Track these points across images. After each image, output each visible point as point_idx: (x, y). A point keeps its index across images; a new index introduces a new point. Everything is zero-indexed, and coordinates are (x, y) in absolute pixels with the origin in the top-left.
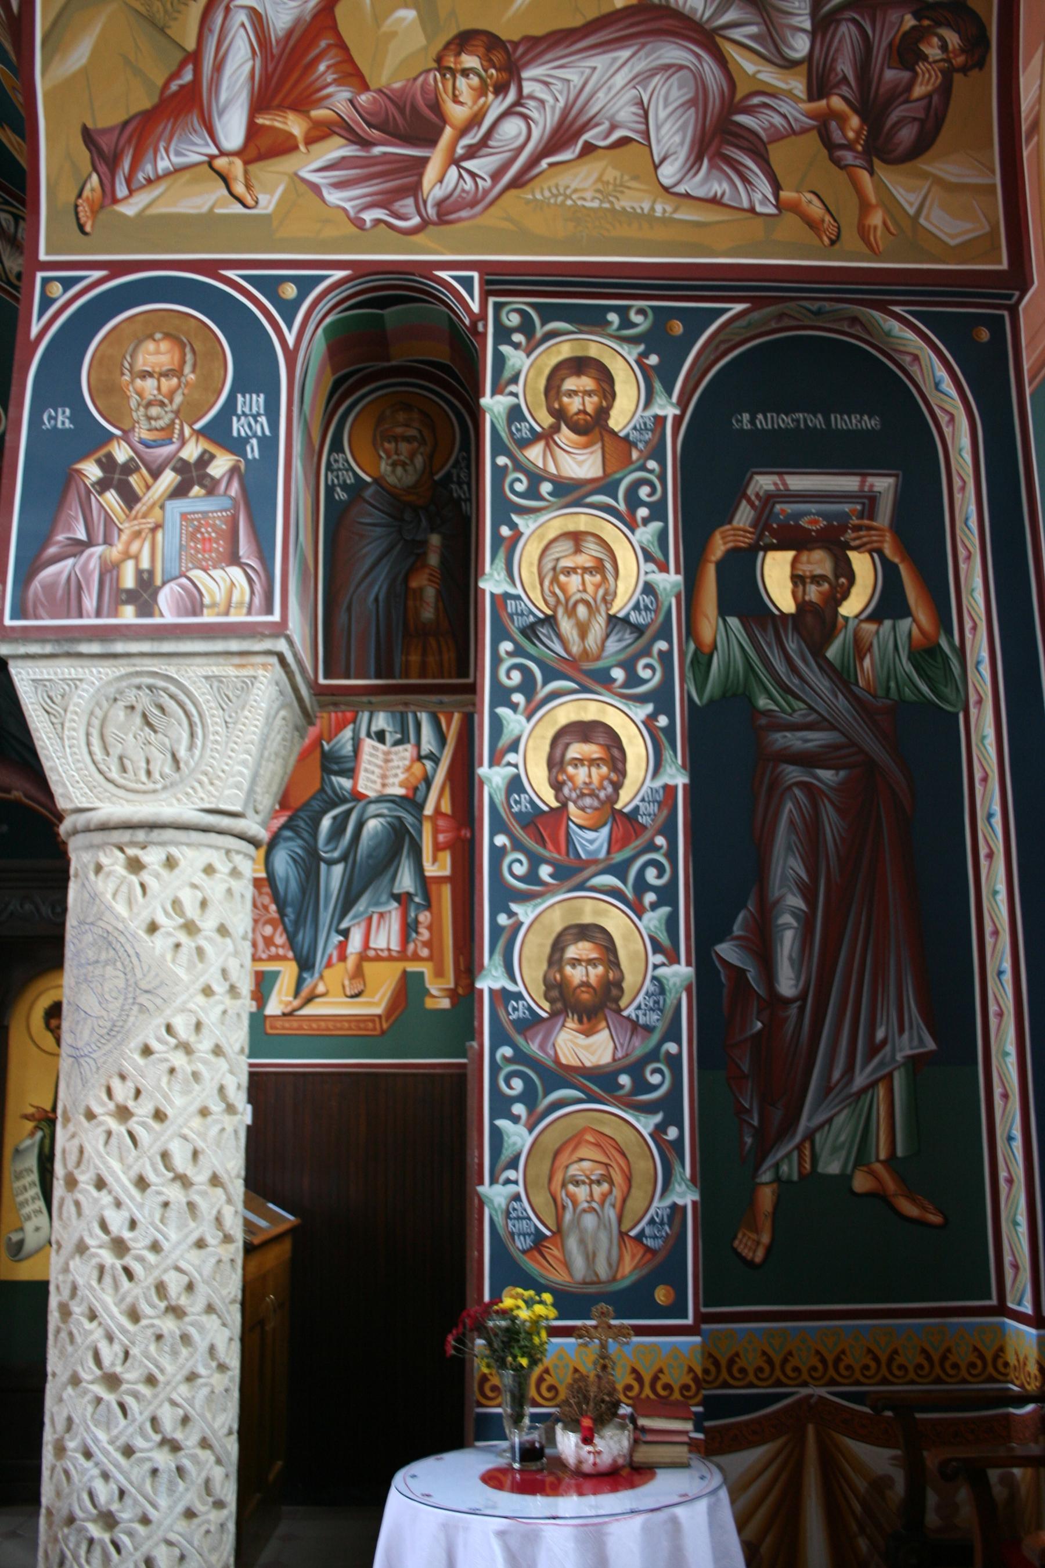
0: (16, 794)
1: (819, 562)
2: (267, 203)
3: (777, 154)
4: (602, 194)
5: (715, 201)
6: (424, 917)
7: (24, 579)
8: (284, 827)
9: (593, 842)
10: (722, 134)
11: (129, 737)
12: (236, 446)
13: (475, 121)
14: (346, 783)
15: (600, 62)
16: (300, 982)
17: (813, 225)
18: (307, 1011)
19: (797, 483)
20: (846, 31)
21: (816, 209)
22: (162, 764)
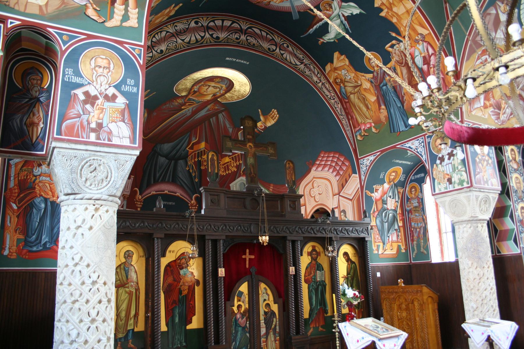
0: (178, 194)
6: (400, 234)
7: (475, 178)
8: (378, 215)
14: (386, 206)
16: (383, 247)
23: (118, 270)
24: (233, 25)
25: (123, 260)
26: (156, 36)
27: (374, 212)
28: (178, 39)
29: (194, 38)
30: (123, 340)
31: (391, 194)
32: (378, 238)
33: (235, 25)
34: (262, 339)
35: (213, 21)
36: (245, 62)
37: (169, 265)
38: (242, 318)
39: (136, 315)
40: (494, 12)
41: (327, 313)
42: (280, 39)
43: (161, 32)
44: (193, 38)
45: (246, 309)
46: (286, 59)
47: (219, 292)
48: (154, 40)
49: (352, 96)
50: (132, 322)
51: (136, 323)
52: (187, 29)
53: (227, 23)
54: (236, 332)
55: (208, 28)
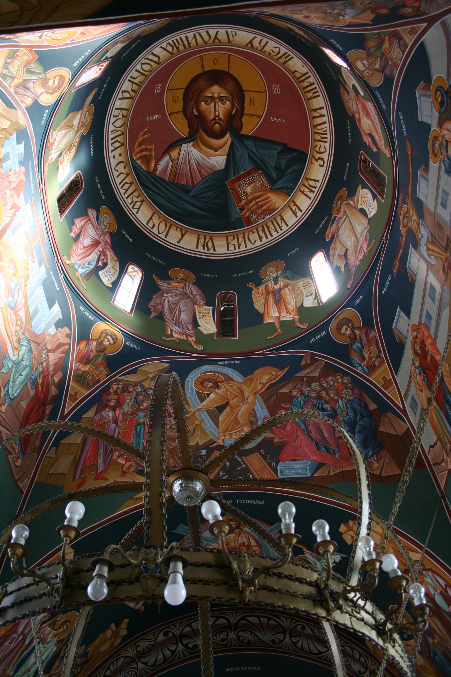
24: (217, 623)
28: (139, 664)
29: (162, 656)
33: (222, 621)
35: (190, 625)
42: (289, 621)
43: (117, 660)
44: (161, 657)
46: (302, 649)
52: (153, 646)
55: (183, 636)
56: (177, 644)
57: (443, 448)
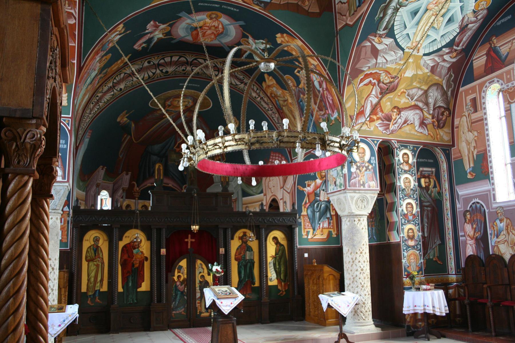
0: (170, 185)
1: (427, 180)
2: (372, 129)
3: (428, 126)
4: (410, 131)
5: (421, 133)
6: (331, 221)
7: (349, 182)
9: (411, 218)
10: (422, 124)
11: (360, 204)
12: (372, 164)
13: (395, 119)
14: (318, 198)
15: (410, 112)
16: (313, 233)
17: (432, 137)
18: (315, 237)
19: (425, 169)
20: (436, 111)
21: (432, 135)
22: (363, 206)
23: (89, 250)
25: (93, 243)
26: (117, 78)
27: (306, 203)
28: (134, 78)
30: (92, 297)
31: (324, 188)
32: (308, 226)
33: (182, 59)
34: (197, 301)
35: (163, 59)
36: (196, 85)
37: (125, 247)
38: (181, 285)
39: (102, 280)
40: (369, 44)
41: (254, 284)
43: (120, 74)
44: (146, 75)
45: (184, 279)
47: (164, 267)
48: (115, 81)
49: (284, 108)
50: (98, 284)
51: (101, 285)
52: (141, 68)
53: (175, 59)
54: (176, 295)
55: (159, 65)
56: (156, 69)
57: (349, 9)
